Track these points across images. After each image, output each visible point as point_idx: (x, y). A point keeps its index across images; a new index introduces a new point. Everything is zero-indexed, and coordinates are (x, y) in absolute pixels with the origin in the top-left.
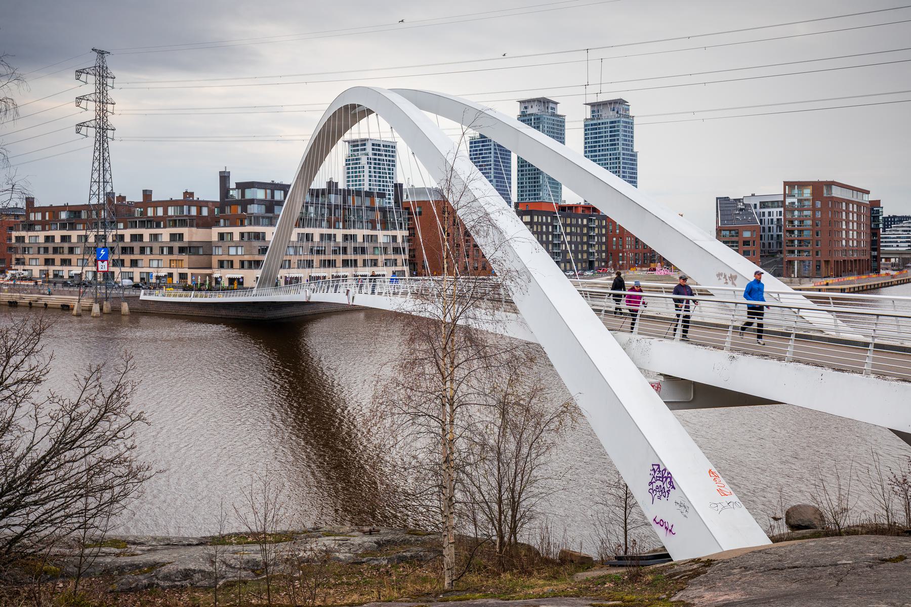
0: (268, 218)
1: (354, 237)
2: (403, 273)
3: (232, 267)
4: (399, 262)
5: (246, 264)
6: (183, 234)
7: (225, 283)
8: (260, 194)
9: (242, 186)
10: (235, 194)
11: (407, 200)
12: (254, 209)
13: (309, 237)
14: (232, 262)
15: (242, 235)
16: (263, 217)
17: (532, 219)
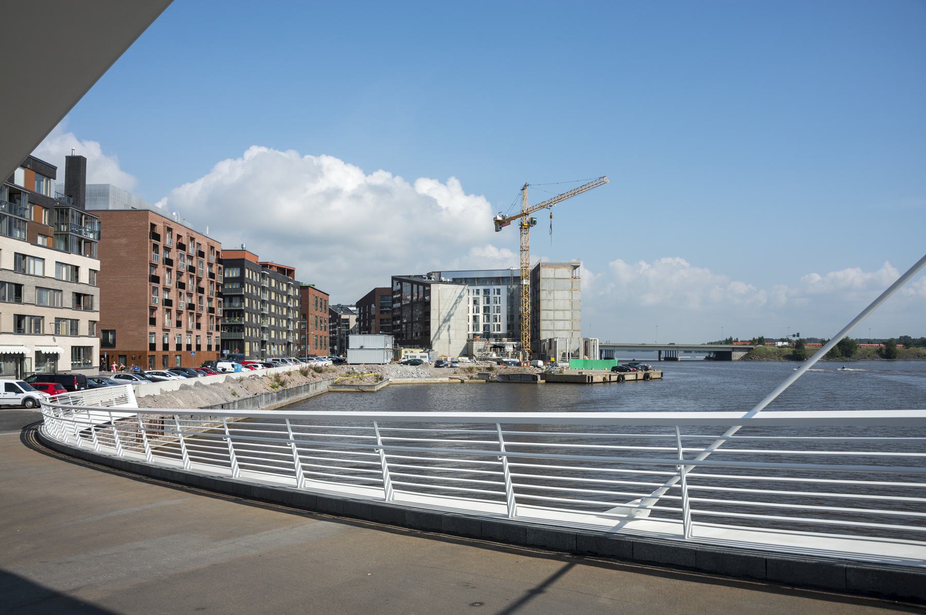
4: (84, 327)
17: (243, 273)
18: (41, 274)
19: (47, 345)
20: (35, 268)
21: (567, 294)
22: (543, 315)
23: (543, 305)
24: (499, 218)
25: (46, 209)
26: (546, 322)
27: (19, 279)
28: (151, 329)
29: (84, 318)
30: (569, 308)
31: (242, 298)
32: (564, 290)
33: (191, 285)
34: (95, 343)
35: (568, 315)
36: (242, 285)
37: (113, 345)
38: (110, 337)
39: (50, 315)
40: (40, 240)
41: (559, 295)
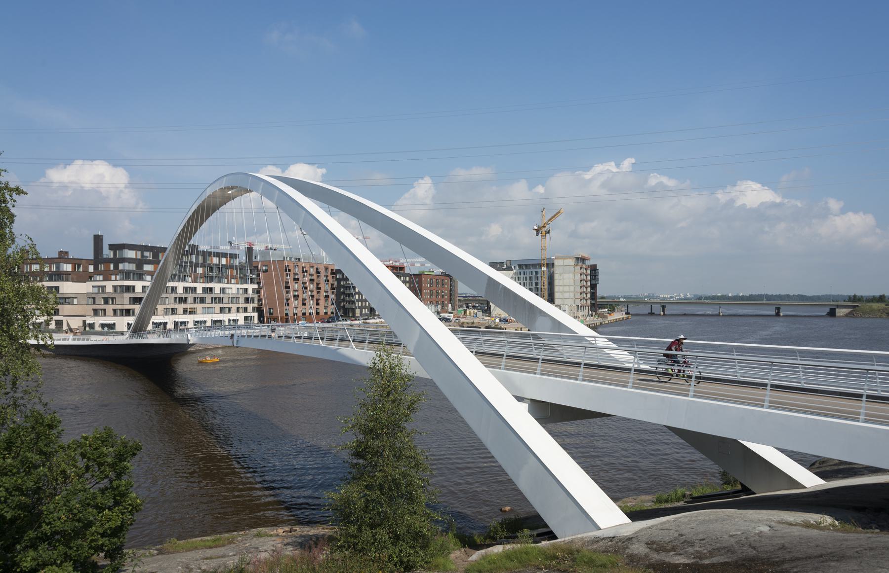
1: (211, 289)
2: (252, 318)
3: (105, 315)
4: (250, 309)
5: (119, 312)
6: (58, 287)
8: (131, 254)
10: (107, 253)
11: (256, 260)
14: (105, 310)
15: (115, 287)
19: (233, 316)
21: (571, 276)
22: (556, 289)
23: (556, 283)
24: (536, 228)
26: (558, 293)
27: (222, 296)
28: (287, 307)
29: (250, 306)
30: (573, 284)
32: (569, 273)
33: (312, 287)
34: (256, 315)
35: (572, 289)
37: (272, 314)
38: (272, 310)
39: (234, 307)
41: (566, 276)
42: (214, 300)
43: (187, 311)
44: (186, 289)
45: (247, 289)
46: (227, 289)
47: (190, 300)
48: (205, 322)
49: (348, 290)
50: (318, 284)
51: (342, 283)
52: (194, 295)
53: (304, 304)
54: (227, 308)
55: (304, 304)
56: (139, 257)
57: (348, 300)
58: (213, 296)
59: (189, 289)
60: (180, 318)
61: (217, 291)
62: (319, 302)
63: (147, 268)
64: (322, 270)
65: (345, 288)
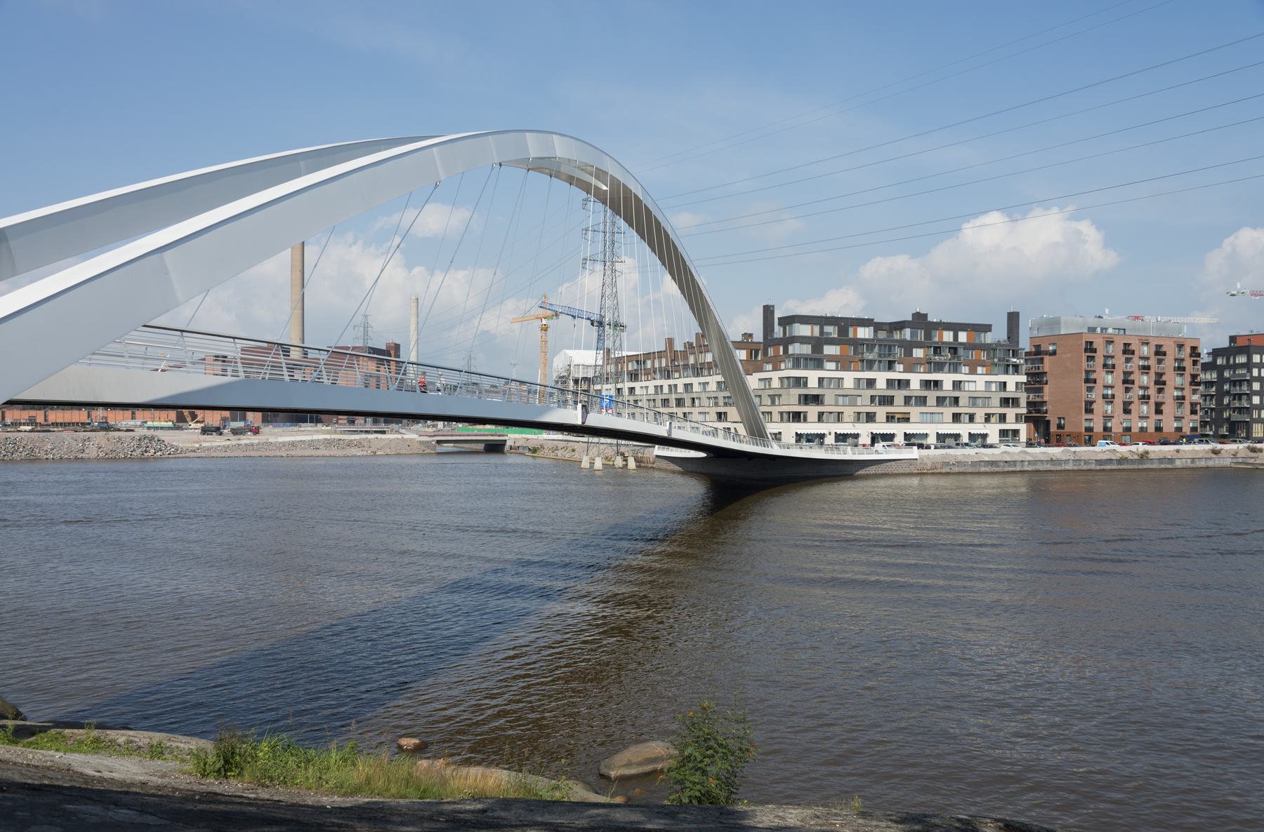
0: (815, 359)
1: (937, 384)
2: (1016, 433)
7: (965, 439)
8: (804, 330)
9: (787, 321)
12: (795, 349)
13: (871, 383)
16: (811, 359)
17: (1250, 358)
18: (974, 389)
20: (967, 387)
25: (984, 350)
27: (956, 394)
28: (1089, 416)
29: (1011, 413)
31: (1249, 383)
36: (1250, 371)
38: (1062, 422)
40: (980, 370)
42: (940, 401)
43: (893, 417)
44: (890, 383)
45: (1005, 383)
46: (966, 384)
47: (932, 400)
48: (926, 435)
49: (1238, 388)
50: (1159, 375)
51: (1226, 374)
52: (905, 393)
53: (1127, 411)
54: (966, 414)
55: (1127, 411)
56: (817, 332)
57: (1237, 405)
58: (940, 394)
59: (896, 382)
60: (882, 428)
61: (948, 386)
62: (1163, 407)
63: (829, 350)
64: (1170, 349)
65: (1232, 383)
